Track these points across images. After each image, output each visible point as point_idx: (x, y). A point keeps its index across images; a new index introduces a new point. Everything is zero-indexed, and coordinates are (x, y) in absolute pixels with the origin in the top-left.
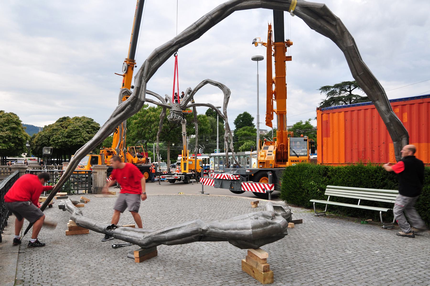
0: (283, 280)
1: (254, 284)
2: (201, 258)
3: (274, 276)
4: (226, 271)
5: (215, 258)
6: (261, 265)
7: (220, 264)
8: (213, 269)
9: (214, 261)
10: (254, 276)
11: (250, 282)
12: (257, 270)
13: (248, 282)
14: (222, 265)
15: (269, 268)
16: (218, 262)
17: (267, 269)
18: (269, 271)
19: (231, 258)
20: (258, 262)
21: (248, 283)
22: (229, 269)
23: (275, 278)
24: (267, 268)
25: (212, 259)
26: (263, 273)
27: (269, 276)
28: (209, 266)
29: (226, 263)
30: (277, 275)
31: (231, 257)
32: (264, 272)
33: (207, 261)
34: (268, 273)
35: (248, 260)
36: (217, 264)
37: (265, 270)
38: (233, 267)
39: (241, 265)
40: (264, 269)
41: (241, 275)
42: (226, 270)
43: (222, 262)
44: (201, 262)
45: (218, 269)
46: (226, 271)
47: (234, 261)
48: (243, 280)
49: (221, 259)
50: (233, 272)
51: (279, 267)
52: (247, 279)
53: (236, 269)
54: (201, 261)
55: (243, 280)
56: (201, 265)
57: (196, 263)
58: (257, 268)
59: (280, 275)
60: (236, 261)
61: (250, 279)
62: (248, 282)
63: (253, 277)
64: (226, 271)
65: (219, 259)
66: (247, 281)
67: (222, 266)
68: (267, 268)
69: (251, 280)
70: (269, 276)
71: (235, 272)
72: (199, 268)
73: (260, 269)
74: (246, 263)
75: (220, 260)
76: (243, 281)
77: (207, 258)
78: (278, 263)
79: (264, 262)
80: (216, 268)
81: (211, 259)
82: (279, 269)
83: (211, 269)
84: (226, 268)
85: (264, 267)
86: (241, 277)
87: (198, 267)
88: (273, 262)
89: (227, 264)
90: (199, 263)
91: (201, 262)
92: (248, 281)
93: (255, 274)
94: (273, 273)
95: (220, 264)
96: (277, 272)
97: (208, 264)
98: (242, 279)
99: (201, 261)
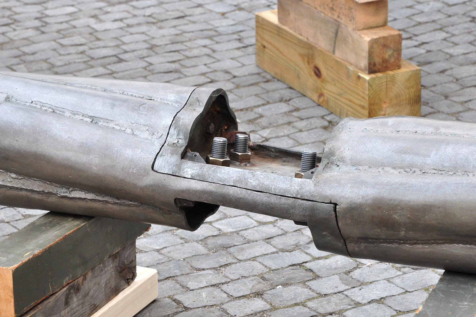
0: (469, 109)
1: (321, 131)
2: (39, 8)
3: (425, 93)
4: (176, 75)
5: (116, 8)
6: (356, 35)
7: (143, 37)
8: (104, 66)
9: (108, 25)
10: (321, 95)
11: (302, 124)
12: (337, 62)
13: (289, 123)
14: (154, 42)
15: (398, 51)
16: (133, 30)
17: (388, 53)
18: (399, 67)
19: (199, 10)
20: (343, 20)
21: (286, 130)
22: (187, 63)
23: (427, 104)
24: (390, 52)
25: (97, 12)
26: (367, 77)
27: (395, 90)
28: (81, 48)
29: (174, 31)
30: (438, 89)
31: (200, 6)
32: (372, 70)
33: (74, 23)
34: (393, 78)
35: (292, 16)
36: (125, 39)
37: (377, 60)
38: (209, 52)
39: (253, 41)
40: (370, 54)
41: (254, 90)
42: (173, 66)
43: (154, 31)
44: (37, 28)
45: (131, 65)
46: (176, 71)
47: (216, 23)
48: (261, 116)
49: (148, 12)
50: (212, 76)
51: (451, 51)
52: (284, 107)
53: (228, 64)
54: (37, 23)
55: (261, 116)
56: (41, 46)
57: (11, 35)
58: (338, 55)
59: (454, 86)
60: (225, 22)
61: (297, 110)
62: (289, 123)
63: (315, 97)
64: (176, 71)
65: (136, 12)
66: (281, 122)
67: (152, 48)
68: (390, 52)
69: (302, 114)
70: (395, 90)
71: (220, 76)
72: (32, 58)
73: (352, 58)
74: (277, 31)
75: (141, 19)
76: (263, 121)
77: (70, 10)
78: (450, 29)
79: (372, 20)
80: (121, 61)
81: (95, 17)
82: (451, 56)
83: (92, 63)
84: (176, 57)
85: (373, 43)
86: (252, 101)
87: (25, 54)
88: (420, 24)
89: (179, 39)
90: (30, 33)
91: (37, 28)
92: (286, 119)
93: (329, 87)
94: (416, 76)
95: (143, 37)
96: (443, 72)
97: (77, 39)
98: (260, 110)
99: (37, 23)
